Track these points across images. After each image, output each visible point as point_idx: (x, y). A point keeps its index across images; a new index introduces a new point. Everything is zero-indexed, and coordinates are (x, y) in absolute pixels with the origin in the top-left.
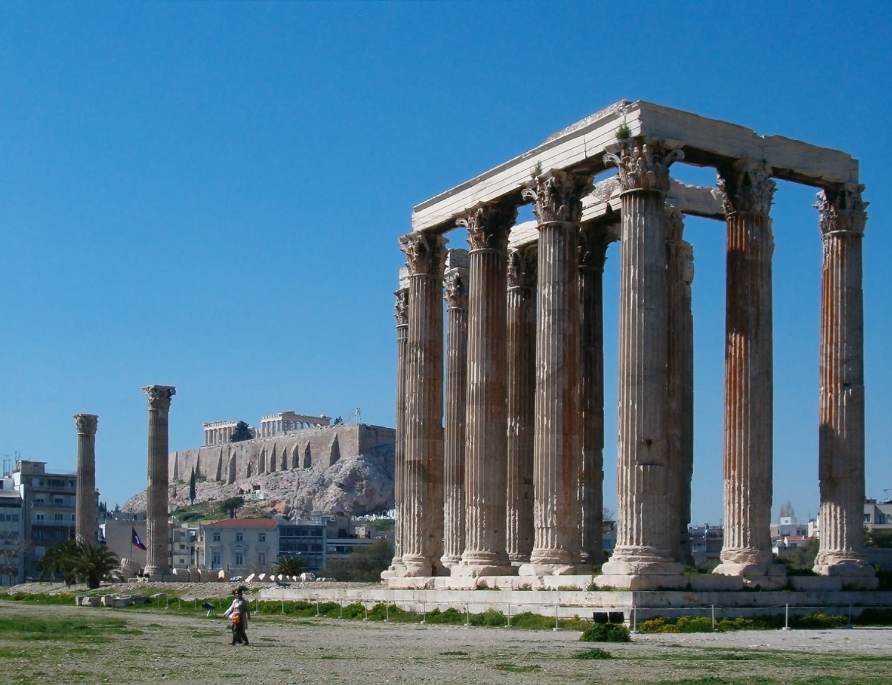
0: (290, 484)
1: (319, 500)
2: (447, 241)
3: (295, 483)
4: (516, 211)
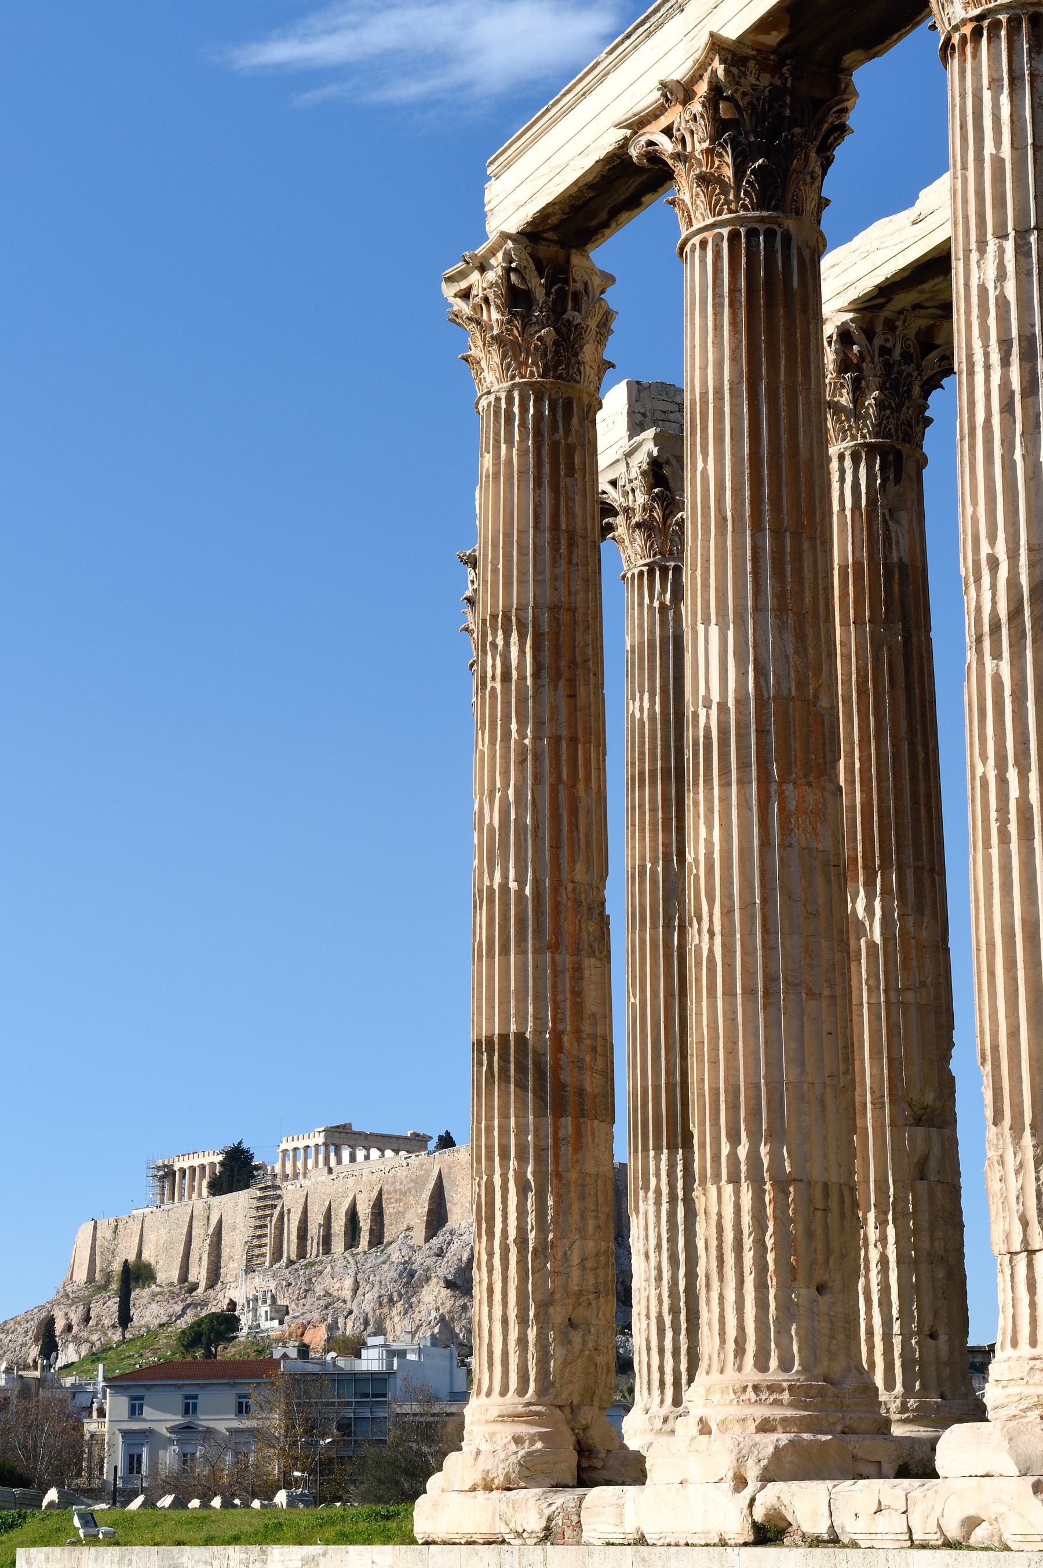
2: (609, 279)
3: (348, 1282)
4: (849, 84)
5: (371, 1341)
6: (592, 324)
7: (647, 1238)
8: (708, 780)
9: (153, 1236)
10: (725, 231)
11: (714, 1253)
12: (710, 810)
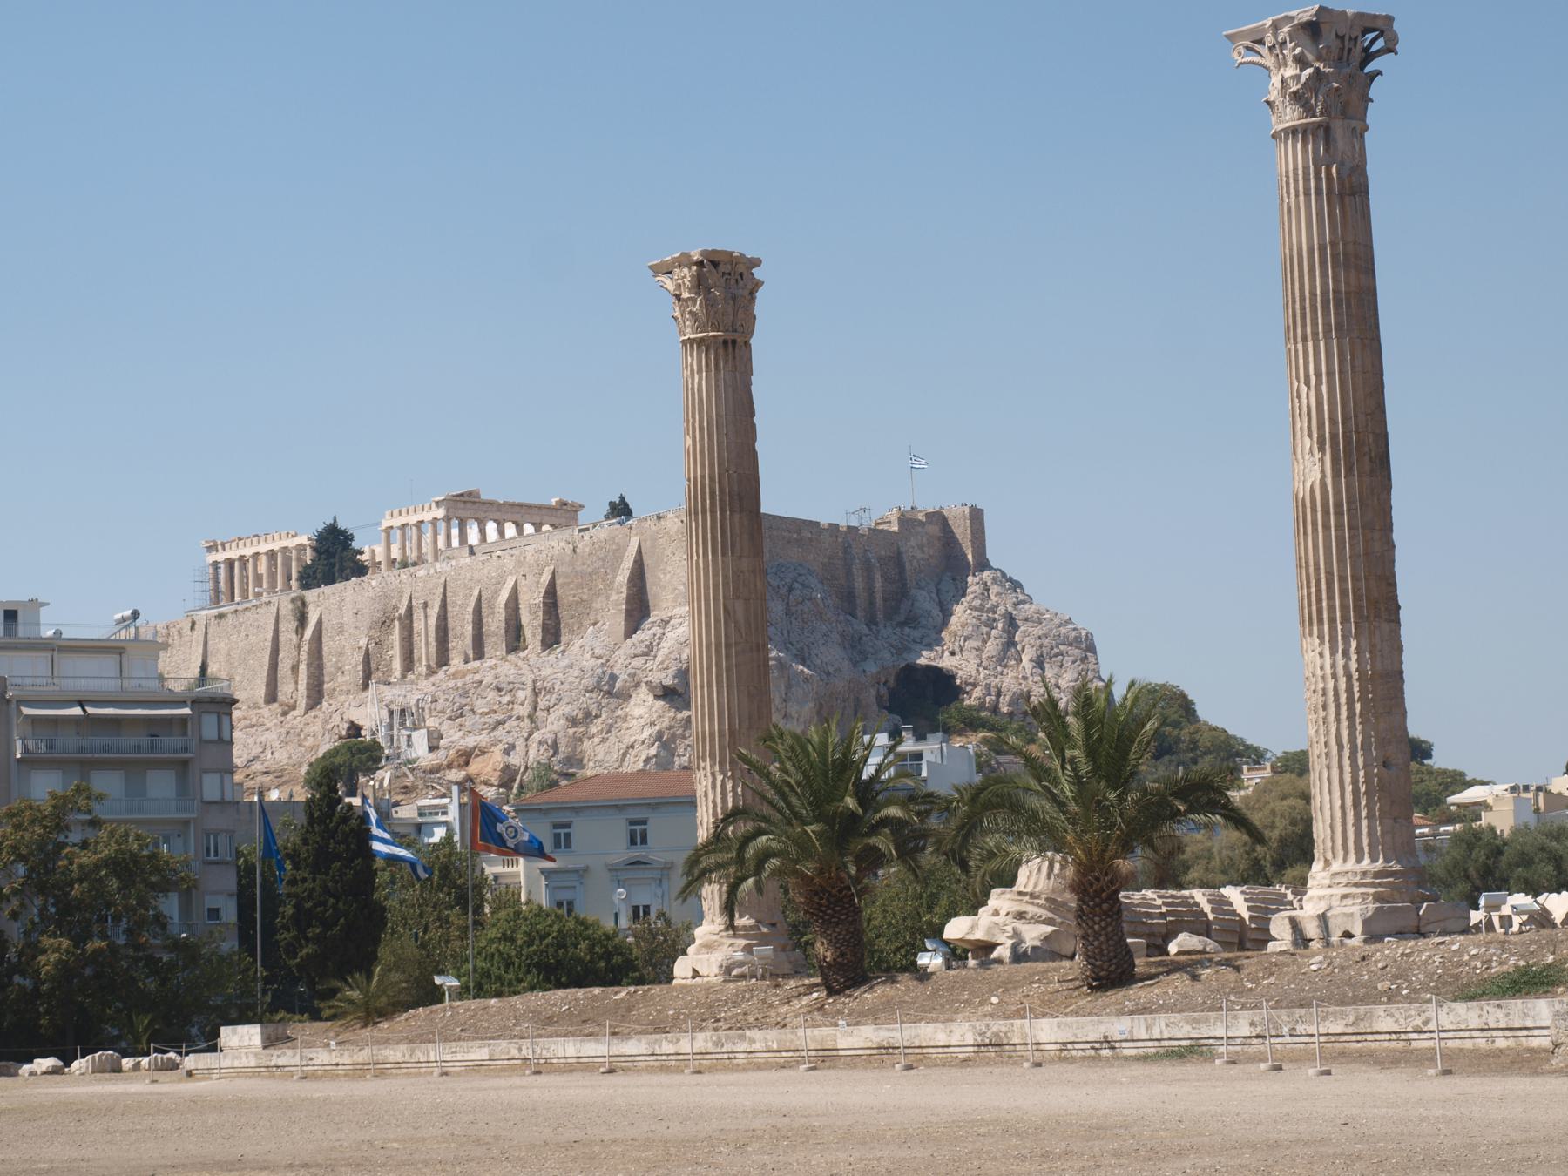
0: (507, 698)
1: (604, 740)
9: (222, 645)
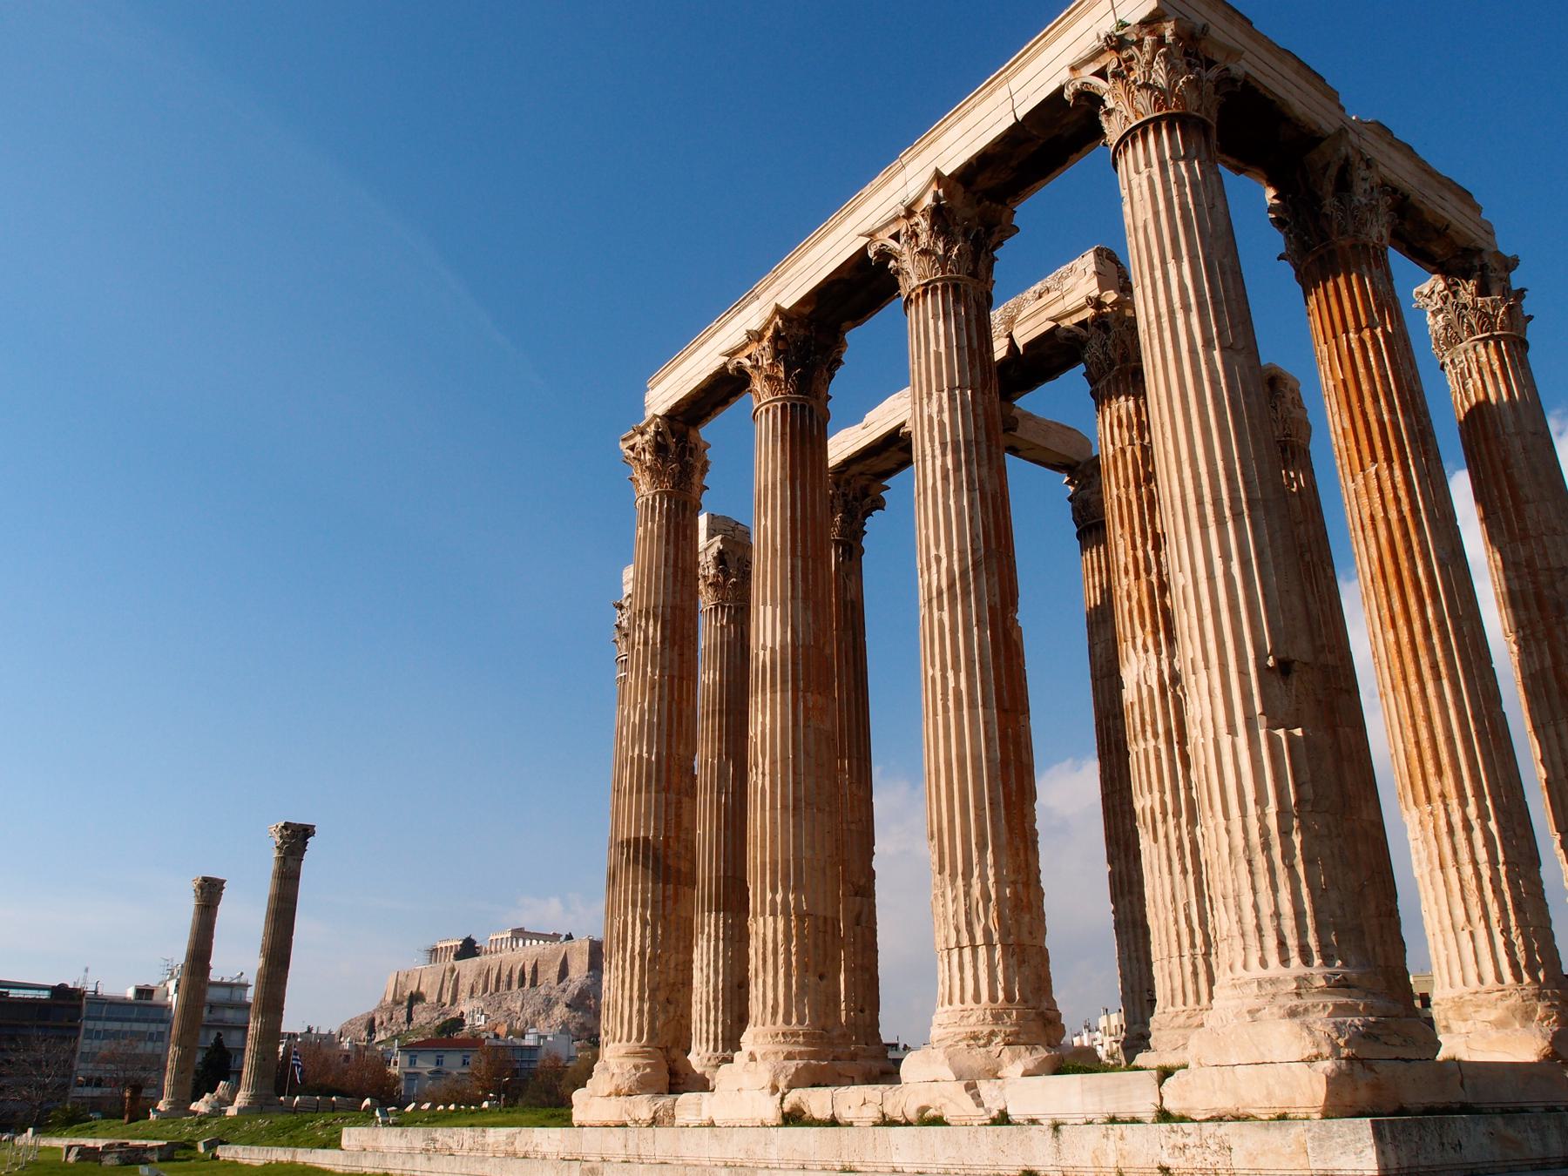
3: (519, 1004)
5: (530, 1031)
6: (699, 465)
7: (702, 960)
8: (764, 690)
10: (779, 404)
11: (760, 956)
12: (764, 706)
